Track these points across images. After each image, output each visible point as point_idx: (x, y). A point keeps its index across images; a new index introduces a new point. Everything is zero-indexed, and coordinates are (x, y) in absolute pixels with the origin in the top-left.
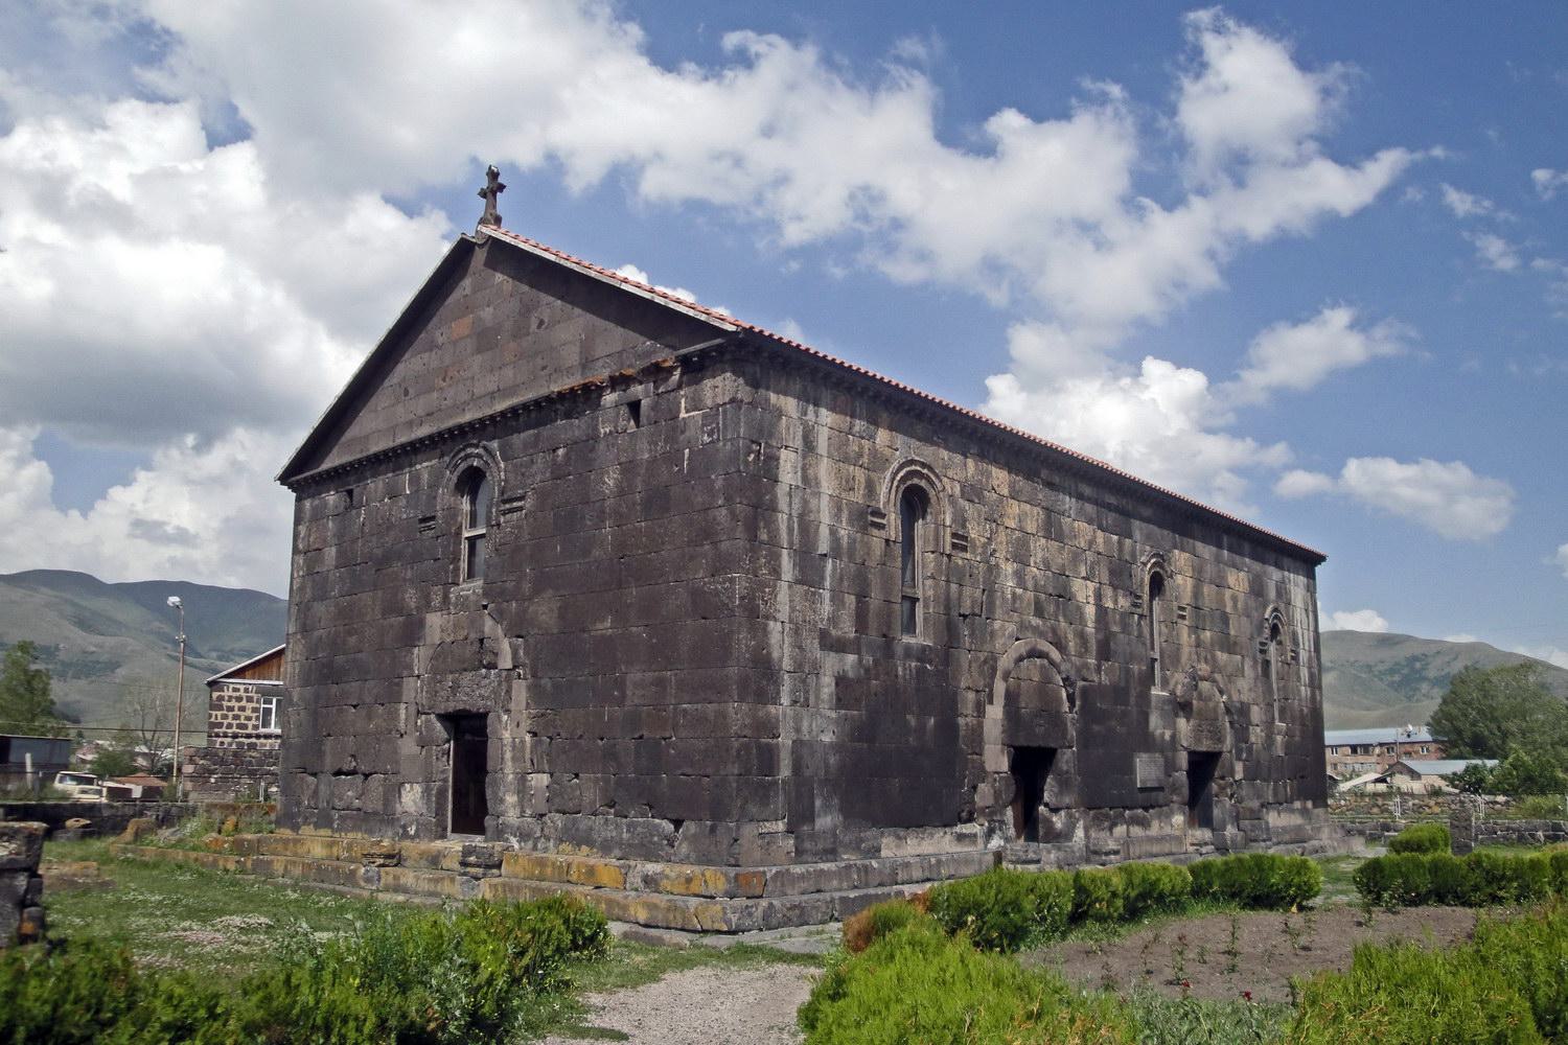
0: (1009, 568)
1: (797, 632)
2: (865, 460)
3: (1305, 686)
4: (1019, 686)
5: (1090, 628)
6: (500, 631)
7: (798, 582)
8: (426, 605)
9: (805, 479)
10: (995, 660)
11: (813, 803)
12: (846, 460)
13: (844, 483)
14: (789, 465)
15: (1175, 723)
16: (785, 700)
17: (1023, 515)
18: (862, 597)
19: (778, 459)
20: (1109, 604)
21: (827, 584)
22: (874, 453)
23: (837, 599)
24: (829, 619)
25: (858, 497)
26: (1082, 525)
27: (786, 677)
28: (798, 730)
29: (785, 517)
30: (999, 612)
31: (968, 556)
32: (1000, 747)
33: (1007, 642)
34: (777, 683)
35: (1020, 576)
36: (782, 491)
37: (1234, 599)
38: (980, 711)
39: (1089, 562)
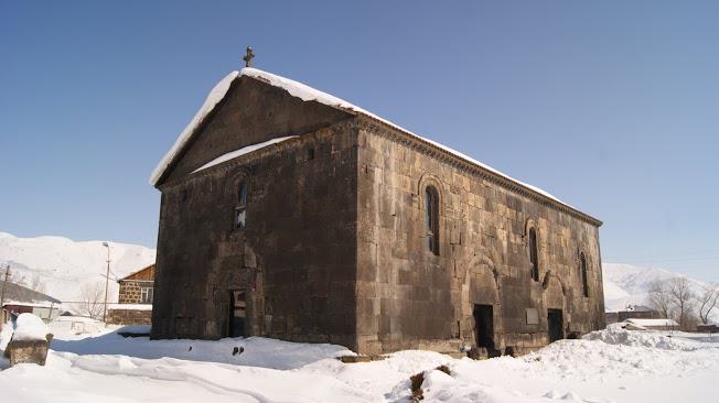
0: (471, 223)
1: (382, 248)
5: (505, 252)
6: (251, 250)
8: (219, 239)
9: (386, 181)
16: (378, 280)
17: (476, 200)
18: (410, 233)
20: (513, 241)
23: (399, 235)
25: (408, 190)
26: (500, 205)
34: (374, 272)
35: (475, 227)
36: (376, 186)
37: (565, 241)
38: (460, 287)
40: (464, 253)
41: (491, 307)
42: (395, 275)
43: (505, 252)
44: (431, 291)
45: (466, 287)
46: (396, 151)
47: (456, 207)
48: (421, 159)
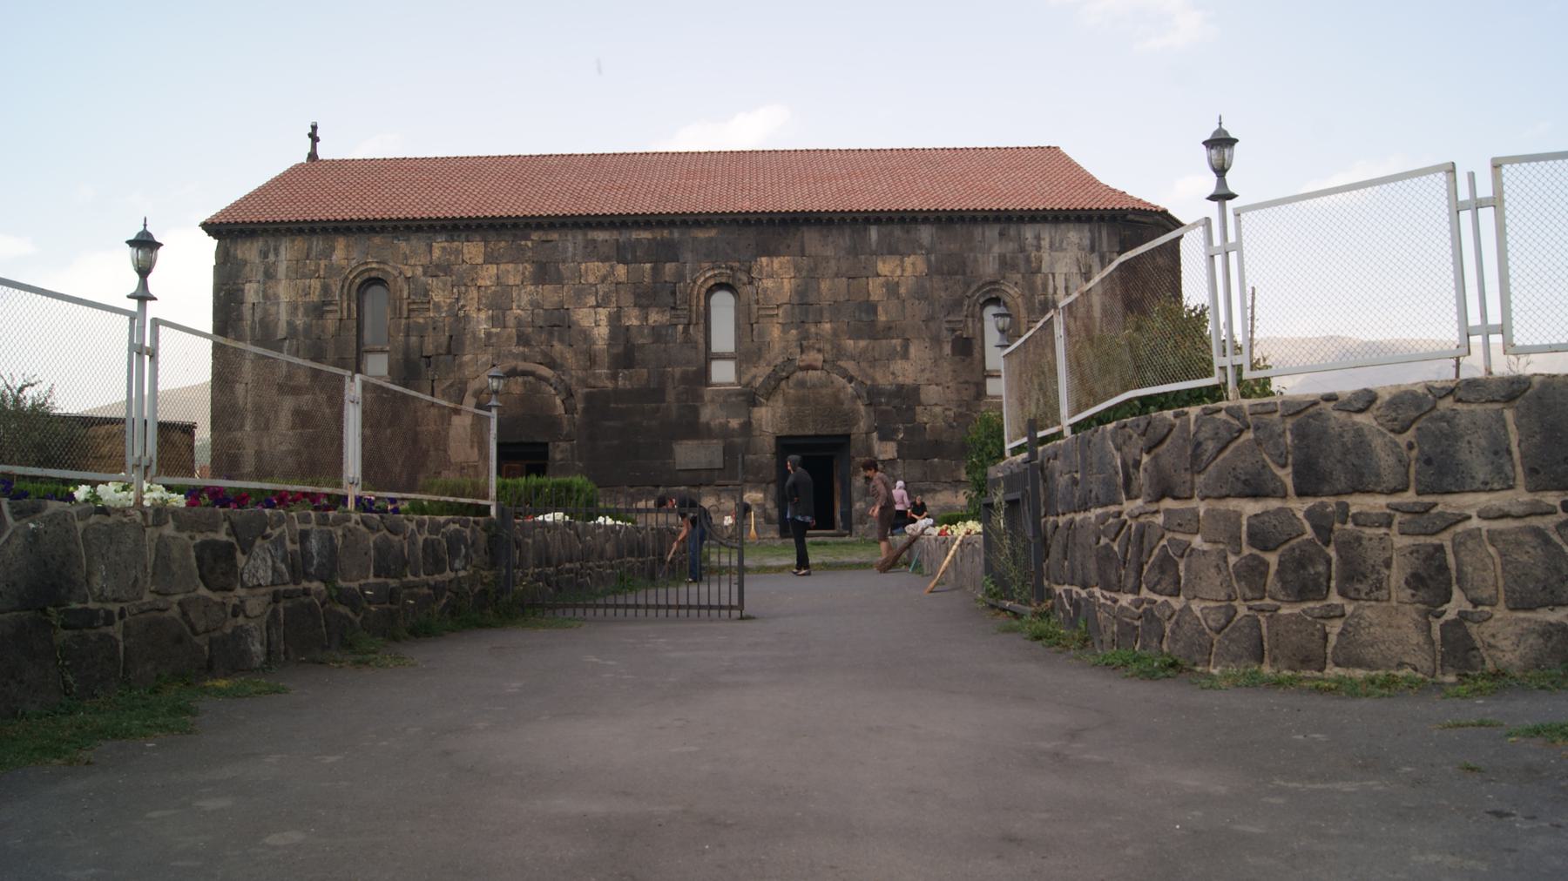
2: (322, 273)
5: (601, 345)
9: (266, 297)
10: (466, 383)
12: (304, 276)
15: (750, 412)
16: (248, 428)
19: (243, 290)
20: (635, 322)
22: (330, 268)
25: (315, 297)
28: (260, 444)
30: (468, 349)
31: (432, 315)
33: (481, 371)
35: (494, 320)
36: (246, 310)
39: (601, 293)
40: (461, 366)
41: (546, 444)
42: (284, 419)
43: (601, 345)
46: (287, 253)
47: (438, 297)
48: (347, 246)
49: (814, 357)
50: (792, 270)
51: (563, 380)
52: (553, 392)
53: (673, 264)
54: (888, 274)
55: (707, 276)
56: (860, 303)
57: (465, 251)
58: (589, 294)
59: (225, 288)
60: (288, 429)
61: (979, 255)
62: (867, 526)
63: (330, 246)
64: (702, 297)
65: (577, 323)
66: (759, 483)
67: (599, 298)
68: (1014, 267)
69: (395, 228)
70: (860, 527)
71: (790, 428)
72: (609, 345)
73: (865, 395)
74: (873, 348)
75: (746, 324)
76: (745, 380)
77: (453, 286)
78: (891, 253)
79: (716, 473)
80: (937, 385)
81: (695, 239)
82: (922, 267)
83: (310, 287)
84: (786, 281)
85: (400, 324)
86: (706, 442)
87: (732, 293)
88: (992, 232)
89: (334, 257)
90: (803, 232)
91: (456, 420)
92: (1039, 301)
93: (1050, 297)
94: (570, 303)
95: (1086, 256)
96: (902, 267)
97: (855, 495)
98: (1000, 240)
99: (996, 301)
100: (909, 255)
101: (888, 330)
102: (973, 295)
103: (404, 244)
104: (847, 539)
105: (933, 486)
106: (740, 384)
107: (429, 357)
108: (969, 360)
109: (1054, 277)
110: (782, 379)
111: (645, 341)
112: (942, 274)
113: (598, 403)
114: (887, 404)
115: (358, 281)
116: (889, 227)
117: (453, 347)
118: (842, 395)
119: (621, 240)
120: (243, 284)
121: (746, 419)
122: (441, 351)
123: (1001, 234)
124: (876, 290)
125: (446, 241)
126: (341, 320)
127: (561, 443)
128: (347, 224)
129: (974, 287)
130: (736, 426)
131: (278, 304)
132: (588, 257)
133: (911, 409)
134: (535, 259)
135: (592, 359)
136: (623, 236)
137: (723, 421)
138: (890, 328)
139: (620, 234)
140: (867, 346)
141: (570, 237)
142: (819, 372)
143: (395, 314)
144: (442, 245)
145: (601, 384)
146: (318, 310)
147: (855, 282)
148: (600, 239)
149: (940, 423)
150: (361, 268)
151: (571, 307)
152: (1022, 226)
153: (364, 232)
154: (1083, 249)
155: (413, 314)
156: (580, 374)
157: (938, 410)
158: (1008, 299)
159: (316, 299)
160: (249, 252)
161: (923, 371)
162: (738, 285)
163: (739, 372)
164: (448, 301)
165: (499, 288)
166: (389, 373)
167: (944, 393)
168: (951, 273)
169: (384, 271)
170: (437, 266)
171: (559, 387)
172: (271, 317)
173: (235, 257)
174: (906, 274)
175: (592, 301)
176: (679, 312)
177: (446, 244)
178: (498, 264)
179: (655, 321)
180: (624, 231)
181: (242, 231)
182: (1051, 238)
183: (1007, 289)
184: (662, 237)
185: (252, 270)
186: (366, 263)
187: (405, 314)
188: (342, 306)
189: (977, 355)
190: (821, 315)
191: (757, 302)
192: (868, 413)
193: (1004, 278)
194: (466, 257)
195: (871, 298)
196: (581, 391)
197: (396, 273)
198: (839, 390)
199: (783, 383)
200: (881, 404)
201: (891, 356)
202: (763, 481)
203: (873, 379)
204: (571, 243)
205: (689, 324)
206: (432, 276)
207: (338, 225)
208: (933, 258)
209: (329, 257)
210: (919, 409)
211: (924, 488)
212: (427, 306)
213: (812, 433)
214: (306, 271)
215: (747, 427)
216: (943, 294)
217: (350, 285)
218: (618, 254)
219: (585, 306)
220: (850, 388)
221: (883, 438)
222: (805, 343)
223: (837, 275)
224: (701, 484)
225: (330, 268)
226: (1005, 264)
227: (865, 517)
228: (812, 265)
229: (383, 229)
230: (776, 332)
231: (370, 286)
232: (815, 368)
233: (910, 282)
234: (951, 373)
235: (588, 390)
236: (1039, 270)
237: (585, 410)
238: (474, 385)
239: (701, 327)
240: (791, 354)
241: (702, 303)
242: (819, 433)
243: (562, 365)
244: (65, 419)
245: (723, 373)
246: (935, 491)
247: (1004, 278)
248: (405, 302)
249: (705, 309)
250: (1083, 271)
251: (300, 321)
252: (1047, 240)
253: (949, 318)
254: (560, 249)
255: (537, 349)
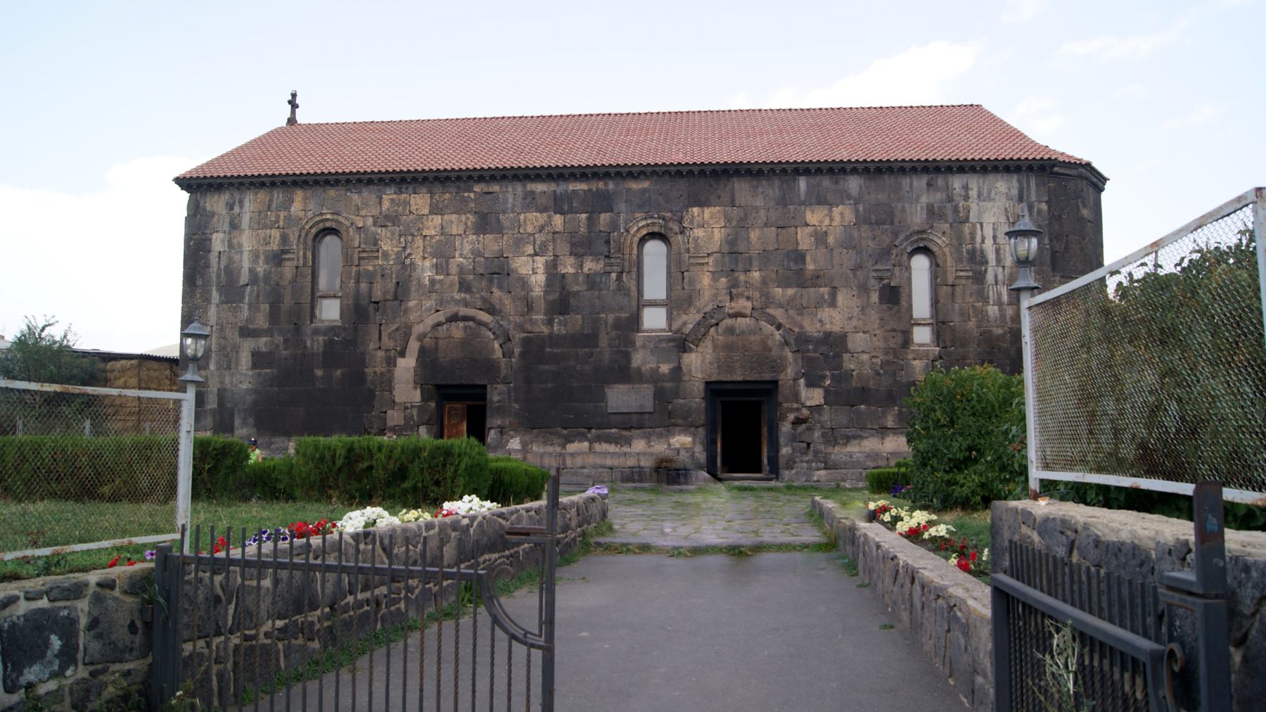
1: (222, 330)
2: (281, 223)
3: (999, 303)
4: (437, 343)
5: (538, 292)
7: (224, 303)
9: (231, 246)
10: (410, 328)
11: (233, 422)
12: (265, 227)
13: (261, 241)
14: (218, 242)
15: (680, 358)
19: (210, 240)
20: (571, 270)
21: (247, 300)
22: (289, 218)
23: (253, 307)
24: (247, 320)
25: (275, 246)
27: (213, 355)
28: (222, 383)
29: (215, 269)
30: (413, 294)
31: (380, 263)
32: (412, 385)
35: (438, 268)
36: (213, 258)
38: (391, 362)
39: (538, 242)
40: (406, 311)
41: (484, 387)
42: (245, 359)
43: (538, 292)
44: (319, 373)
45: (407, 365)
46: (251, 203)
47: (386, 246)
48: (305, 199)
49: (743, 305)
50: (722, 220)
51: (502, 325)
52: (492, 337)
53: (609, 214)
54: (817, 224)
55: (640, 225)
56: (789, 252)
57: (412, 202)
58: (527, 243)
59: (194, 237)
60: (247, 370)
61: (907, 205)
62: (793, 471)
63: (289, 199)
64: (635, 246)
65: (516, 271)
66: (688, 427)
67: (537, 247)
68: (942, 217)
69: (348, 181)
70: (787, 472)
71: (719, 374)
72: (546, 292)
73: (792, 342)
74: (802, 295)
75: (677, 271)
76: (675, 326)
77: (400, 236)
78: (819, 203)
79: (647, 416)
80: (864, 332)
81: (629, 190)
82: (850, 217)
83: (270, 237)
84: (716, 231)
85: (351, 273)
86: (637, 386)
87: (664, 241)
88: (920, 182)
89: (293, 209)
90: (734, 183)
91: (401, 362)
92: (968, 251)
93: (978, 246)
94: (509, 252)
95: (1014, 206)
96: (830, 217)
97: (782, 440)
98: (928, 190)
99: (926, 251)
100: (837, 206)
101: (816, 280)
102: (901, 244)
103: (355, 198)
104: (773, 483)
105: (859, 432)
106: (671, 331)
107: (377, 303)
108: (896, 308)
109: (982, 227)
110: (712, 326)
111: (580, 288)
112: (871, 223)
113: (534, 348)
114: (815, 351)
115: (314, 231)
116: (818, 178)
117: (400, 293)
118: (770, 342)
119: (558, 192)
120: (211, 234)
121: (676, 365)
122: (388, 297)
123: (929, 185)
124: (804, 239)
125: (395, 193)
126: (297, 267)
127: (498, 386)
128: (304, 178)
129: (902, 237)
130: (667, 371)
131: (242, 252)
132: (526, 208)
133: (838, 356)
134: (477, 210)
135: (529, 306)
136: (561, 188)
137: (654, 366)
138: (818, 277)
139: (558, 185)
140: (795, 294)
141: (510, 189)
142: (748, 319)
143: (347, 262)
144: (391, 197)
145: (537, 330)
146: (277, 258)
147: (784, 231)
148: (538, 190)
149: (867, 370)
150: (318, 219)
151: (510, 255)
152: (950, 175)
153: (320, 185)
154: (1012, 199)
155: (363, 262)
156: (518, 319)
157: (865, 357)
158: (935, 249)
159: (275, 248)
160: (217, 203)
161: (850, 318)
162: (669, 234)
163: (670, 318)
164: (396, 249)
165: (442, 238)
166: (341, 318)
167: (871, 341)
168: (879, 223)
169: (337, 221)
170: (386, 217)
171: (498, 332)
172: (235, 265)
173: (204, 209)
174: (835, 224)
175: (530, 250)
176: (612, 260)
177: (394, 196)
178: (442, 215)
179: (589, 269)
180: (561, 183)
181: (210, 185)
182: (979, 188)
183: (936, 240)
184: (597, 189)
185: (219, 221)
186: (321, 214)
187: (356, 263)
188: (299, 253)
189: (904, 303)
190: (750, 264)
191: (688, 251)
192: (795, 360)
193: (932, 227)
194: (413, 208)
195: (800, 247)
196: (518, 336)
197: (348, 224)
198: (768, 338)
199: (712, 330)
200: (808, 351)
201: (819, 304)
202: (691, 425)
203: (801, 327)
204: (511, 194)
205: (622, 273)
206: (382, 226)
207: (296, 178)
208: (861, 208)
209: (287, 208)
210: (846, 356)
211: (850, 434)
212: (376, 254)
213: (740, 379)
214: (268, 222)
215: (677, 371)
216: (870, 243)
217: (307, 235)
218: (555, 205)
219: (523, 254)
220: (778, 336)
221: (810, 385)
222: (734, 291)
223: (766, 225)
224: (632, 427)
225: (289, 218)
226: (931, 211)
227: (791, 463)
228: (742, 214)
229: (337, 182)
230: (706, 280)
231: (325, 236)
232: (744, 316)
233: (838, 231)
234: (878, 321)
235: (525, 335)
236: (967, 220)
237: (522, 354)
238: (418, 329)
239: (634, 275)
240: (720, 301)
241: (635, 252)
242: (748, 379)
243: (501, 311)
244: (85, 354)
245: (654, 319)
246: (861, 438)
247: (932, 227)
248: (357, 250)
249: (638, 257)
250: (1011, 220)
251: (261, 269)
252: (976, 189)
253: (878, 267)
254: (501, 200)
255: (478, 295)
